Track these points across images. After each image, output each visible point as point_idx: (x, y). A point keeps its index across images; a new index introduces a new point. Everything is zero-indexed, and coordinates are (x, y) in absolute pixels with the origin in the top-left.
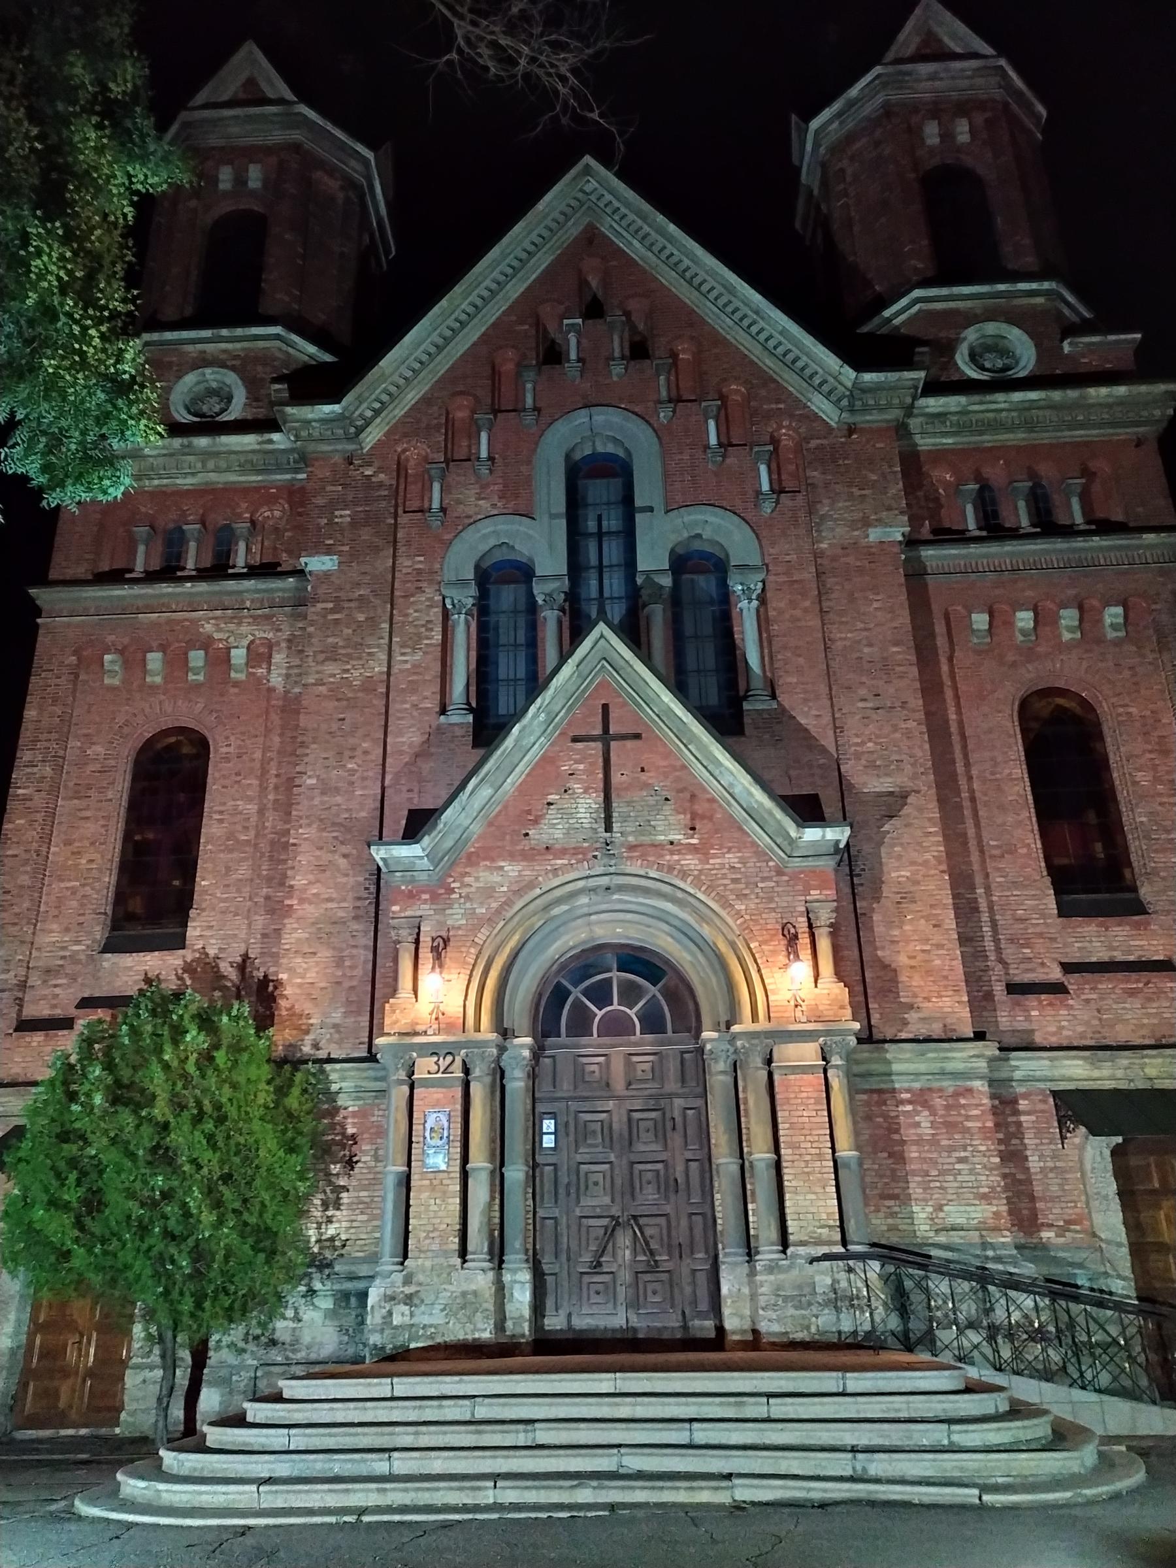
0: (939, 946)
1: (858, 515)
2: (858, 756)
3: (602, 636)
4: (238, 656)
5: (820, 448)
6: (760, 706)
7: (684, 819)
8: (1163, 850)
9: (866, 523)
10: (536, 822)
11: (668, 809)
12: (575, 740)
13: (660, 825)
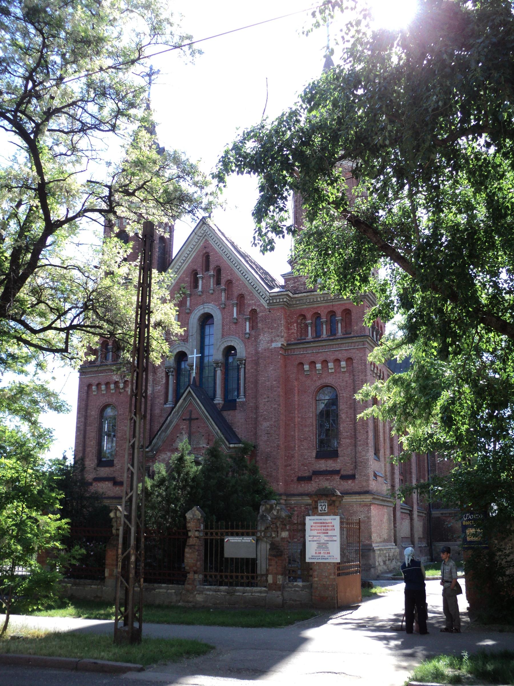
0: (274, 469)
1: (270, 339)
2: (262, 416)
3: (190, 391)
4: (121, 385)
5: (262, 316)
6: (241, 400)
7: (206, 441)
8: (345, 438)
9: (272, 341)
10: (174, 442)
11: (203, 438)
12: (184, 420)
13: (201, 442)
